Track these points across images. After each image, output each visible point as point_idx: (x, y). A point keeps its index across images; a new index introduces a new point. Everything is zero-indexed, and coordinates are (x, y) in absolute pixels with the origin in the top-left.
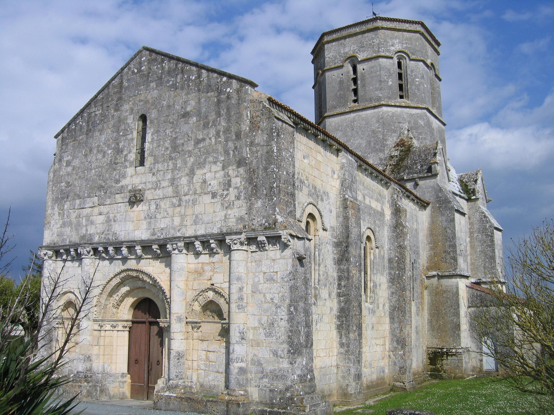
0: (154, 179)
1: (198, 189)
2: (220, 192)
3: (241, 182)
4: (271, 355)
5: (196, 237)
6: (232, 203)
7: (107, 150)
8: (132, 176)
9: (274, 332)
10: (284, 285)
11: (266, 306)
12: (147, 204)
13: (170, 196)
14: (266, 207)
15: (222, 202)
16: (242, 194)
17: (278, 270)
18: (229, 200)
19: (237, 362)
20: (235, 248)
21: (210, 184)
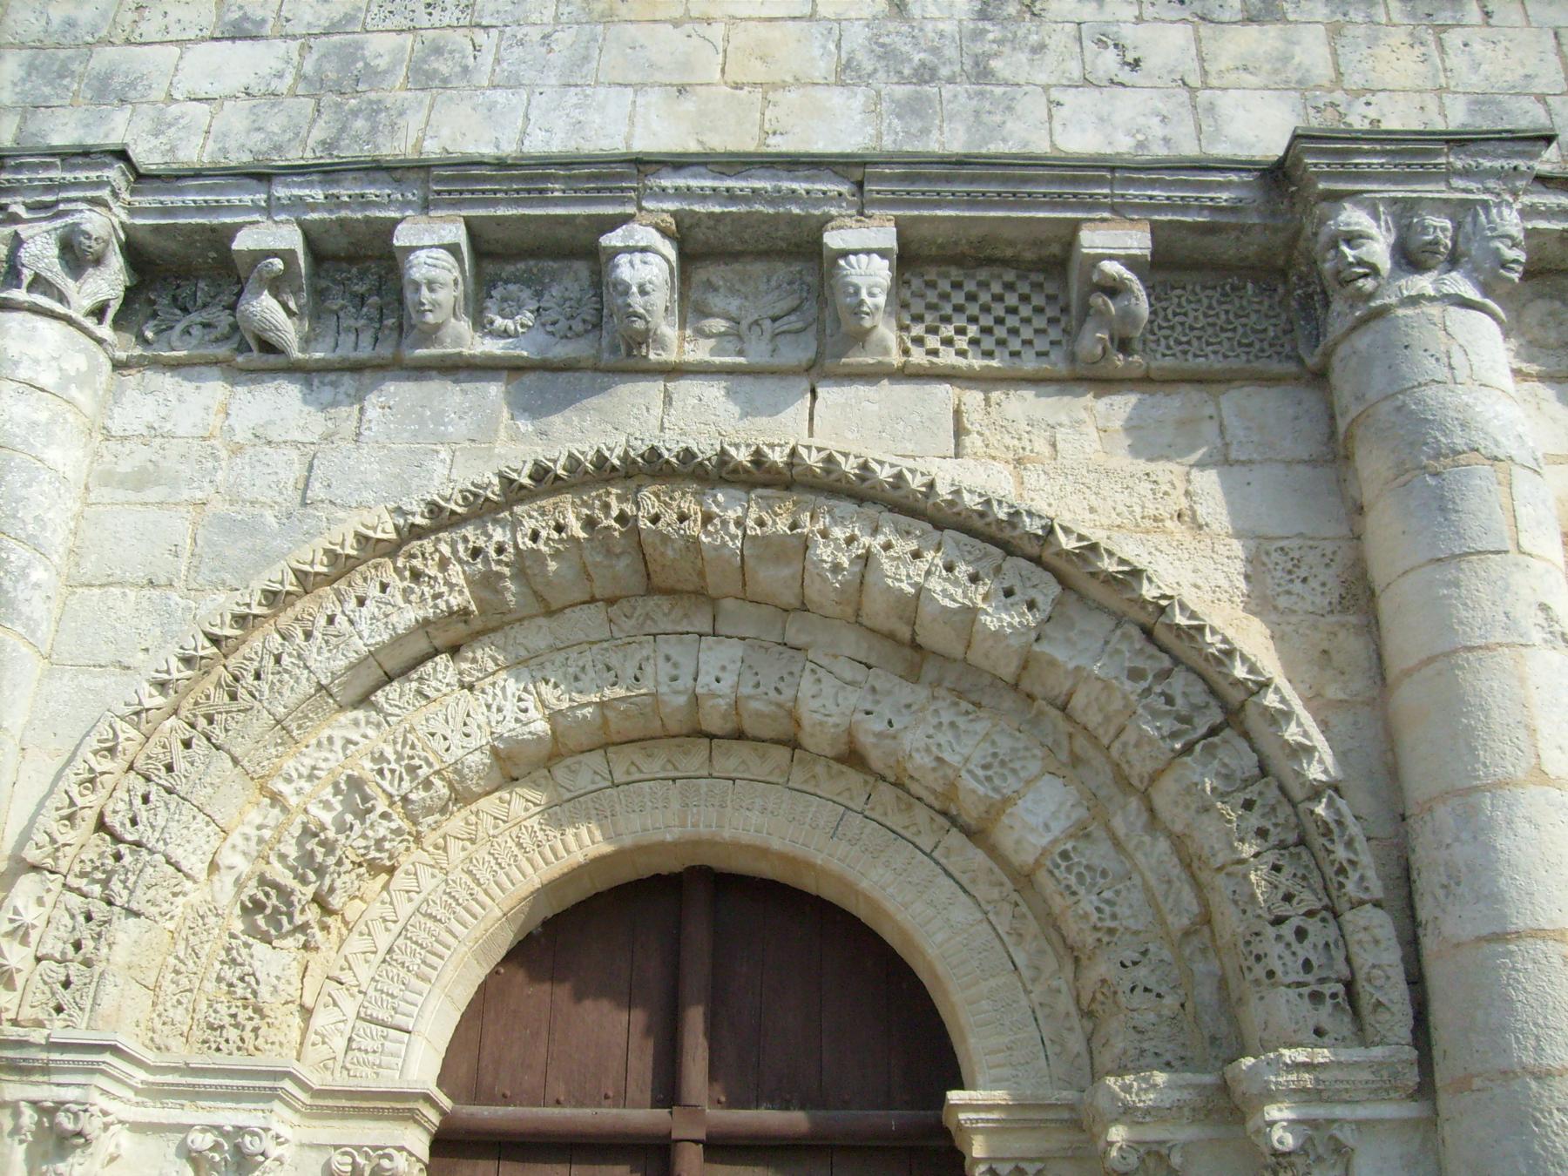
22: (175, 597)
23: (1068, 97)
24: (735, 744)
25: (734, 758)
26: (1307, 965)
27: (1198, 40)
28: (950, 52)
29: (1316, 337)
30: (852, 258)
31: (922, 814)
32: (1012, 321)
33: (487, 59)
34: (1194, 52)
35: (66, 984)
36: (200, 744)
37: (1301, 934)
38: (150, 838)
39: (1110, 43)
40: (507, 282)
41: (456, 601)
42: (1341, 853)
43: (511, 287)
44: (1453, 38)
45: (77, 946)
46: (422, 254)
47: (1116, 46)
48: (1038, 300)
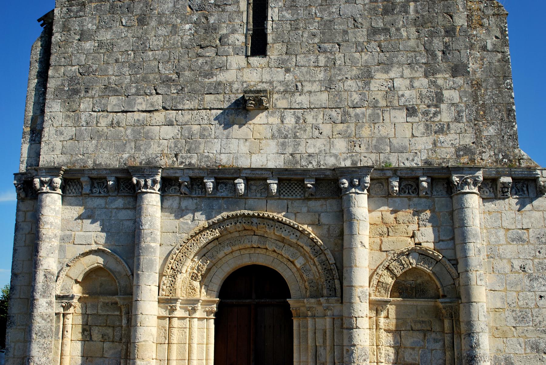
0: (289, 77)
1: (380, 100)
2: (423, 107)
3: (460, 98)
4: (528, 351)
5: (395, 171)
6: (446, 126)
9: (530, 315)
10: (542, 248)
11: (512, 277)
12: (278, 114)
13: (324, 106)
14: (503, 137)
15: (428, 123)
16: (464, 114)
17: (530, 226)
18: (440, 120)
19: (485, 361)
20: (468, 190)
21: (403, 95)
22: (177, 234)
23: (309, 141)
24: (258, 249)
25: (259, 251)
26: (330, 286)
27: (332, 127)
28: (290, 132)
29: (341, 193)
31: (285, 259)
32: (296, 190)
33: (213, 132)
35: (171, 290)
36: (184, 257)
37: (329, 282)
38: (179, 270)
41: (218, 235)
42: (334, 273)
44: (377, 126)
45: (172, 285)
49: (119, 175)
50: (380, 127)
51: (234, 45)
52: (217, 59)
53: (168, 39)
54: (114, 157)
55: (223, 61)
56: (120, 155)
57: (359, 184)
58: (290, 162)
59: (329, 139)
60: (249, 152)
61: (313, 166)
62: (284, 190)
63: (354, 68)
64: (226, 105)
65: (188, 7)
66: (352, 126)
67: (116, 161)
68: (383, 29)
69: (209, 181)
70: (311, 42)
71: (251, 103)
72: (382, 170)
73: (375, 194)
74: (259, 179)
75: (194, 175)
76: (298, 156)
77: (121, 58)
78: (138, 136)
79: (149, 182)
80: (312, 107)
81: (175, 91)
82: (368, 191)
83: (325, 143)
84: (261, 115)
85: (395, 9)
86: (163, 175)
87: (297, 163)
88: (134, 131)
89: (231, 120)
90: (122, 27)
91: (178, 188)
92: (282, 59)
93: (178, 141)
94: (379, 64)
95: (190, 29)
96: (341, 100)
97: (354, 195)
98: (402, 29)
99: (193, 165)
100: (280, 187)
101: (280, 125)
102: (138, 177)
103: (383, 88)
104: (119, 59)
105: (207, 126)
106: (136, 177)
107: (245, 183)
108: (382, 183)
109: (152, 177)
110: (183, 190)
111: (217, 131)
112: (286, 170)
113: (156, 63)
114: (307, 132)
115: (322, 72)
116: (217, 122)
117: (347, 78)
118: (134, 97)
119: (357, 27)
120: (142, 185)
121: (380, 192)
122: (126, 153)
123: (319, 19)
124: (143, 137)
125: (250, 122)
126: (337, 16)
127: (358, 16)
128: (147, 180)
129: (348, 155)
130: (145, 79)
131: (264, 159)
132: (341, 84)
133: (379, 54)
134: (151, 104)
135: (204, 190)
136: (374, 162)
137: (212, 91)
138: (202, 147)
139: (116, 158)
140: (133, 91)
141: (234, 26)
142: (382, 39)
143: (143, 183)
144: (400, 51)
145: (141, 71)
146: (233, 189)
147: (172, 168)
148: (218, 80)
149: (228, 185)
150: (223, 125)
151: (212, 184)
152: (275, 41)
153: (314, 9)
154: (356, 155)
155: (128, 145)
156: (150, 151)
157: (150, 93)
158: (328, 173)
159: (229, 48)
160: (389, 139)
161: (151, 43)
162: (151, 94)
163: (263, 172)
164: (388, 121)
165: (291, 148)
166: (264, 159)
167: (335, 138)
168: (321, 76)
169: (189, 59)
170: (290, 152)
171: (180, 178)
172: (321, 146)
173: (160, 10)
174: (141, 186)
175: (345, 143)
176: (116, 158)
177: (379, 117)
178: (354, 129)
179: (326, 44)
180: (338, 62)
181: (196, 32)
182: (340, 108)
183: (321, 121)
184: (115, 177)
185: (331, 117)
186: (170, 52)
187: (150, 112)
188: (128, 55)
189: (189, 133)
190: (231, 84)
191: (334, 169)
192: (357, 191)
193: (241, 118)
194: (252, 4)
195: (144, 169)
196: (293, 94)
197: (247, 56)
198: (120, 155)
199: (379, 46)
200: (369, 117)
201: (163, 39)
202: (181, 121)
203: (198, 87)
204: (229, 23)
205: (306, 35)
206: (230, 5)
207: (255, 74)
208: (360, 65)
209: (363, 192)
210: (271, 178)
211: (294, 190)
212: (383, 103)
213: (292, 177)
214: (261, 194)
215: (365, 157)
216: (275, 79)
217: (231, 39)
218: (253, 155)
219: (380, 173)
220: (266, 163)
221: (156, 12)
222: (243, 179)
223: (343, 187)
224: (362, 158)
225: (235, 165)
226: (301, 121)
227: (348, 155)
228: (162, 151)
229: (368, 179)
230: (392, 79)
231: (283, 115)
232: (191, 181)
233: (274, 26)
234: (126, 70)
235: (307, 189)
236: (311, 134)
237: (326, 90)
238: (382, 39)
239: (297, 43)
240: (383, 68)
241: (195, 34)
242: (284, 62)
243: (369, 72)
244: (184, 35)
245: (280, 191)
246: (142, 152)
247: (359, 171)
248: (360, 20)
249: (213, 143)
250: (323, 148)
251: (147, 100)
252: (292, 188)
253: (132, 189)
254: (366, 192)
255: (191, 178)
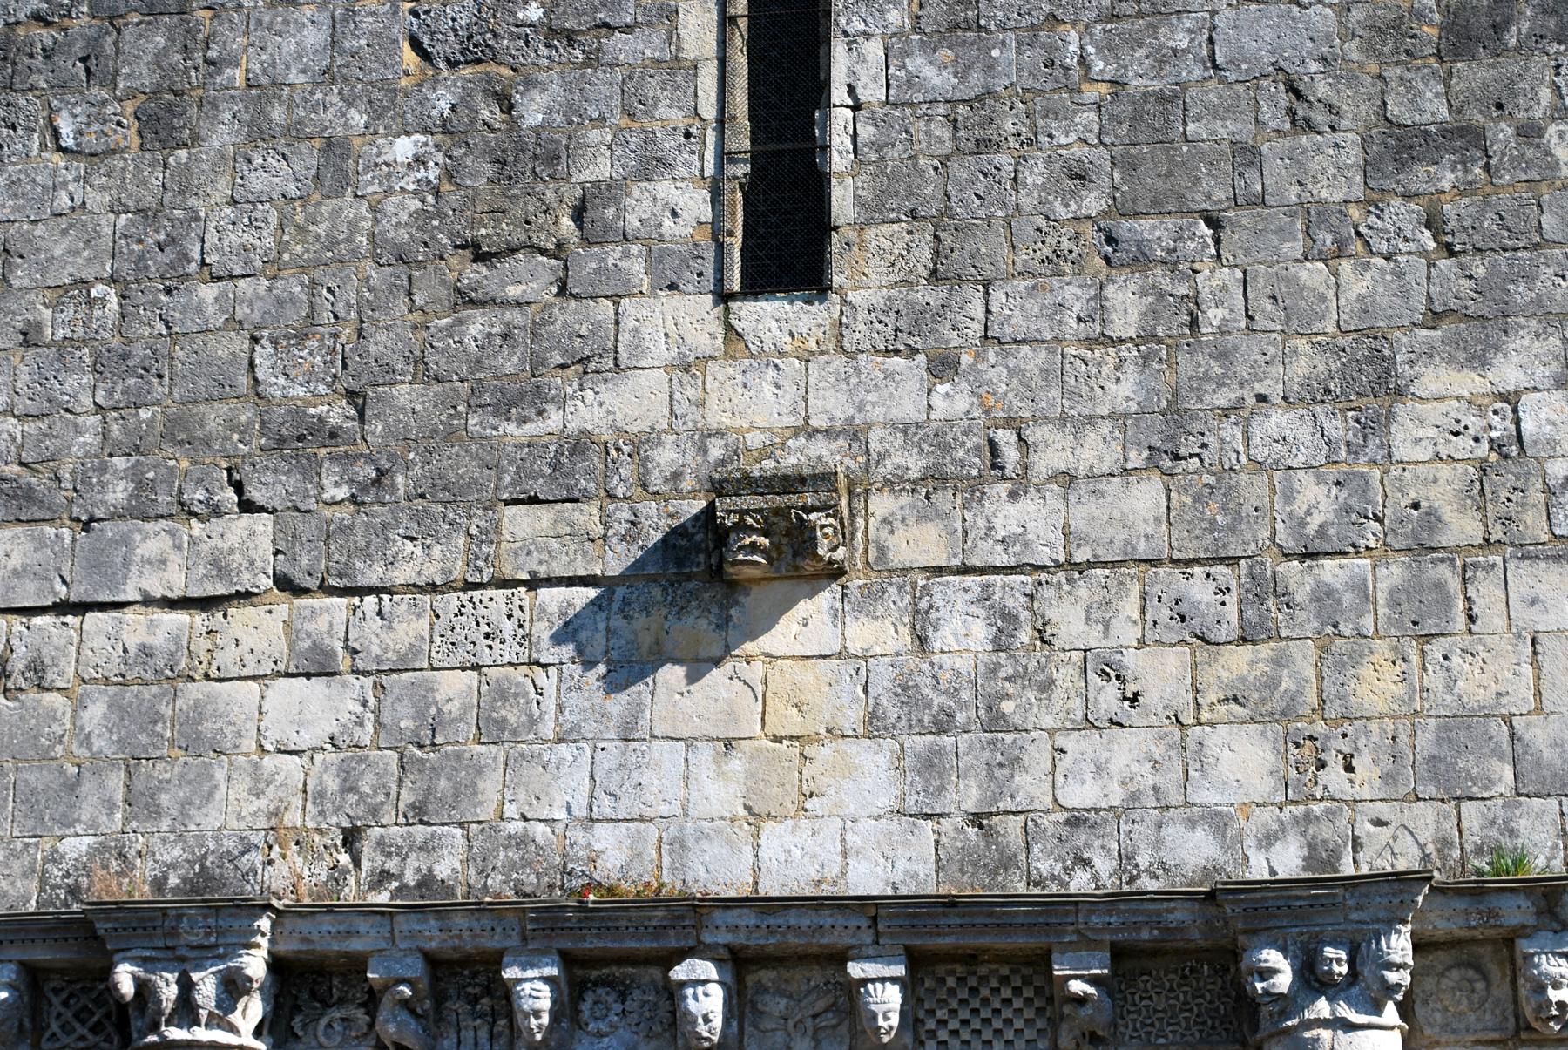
0: (952, 401)
1: (1447, 513)
7: (370, 131)
8: (686, 366)
12: (896, 600)
13: (1142, 550)
23: (1068, 742)
27: (1194, 666)
28: (966, 695)
29: (1255, 1028)
30: (870, 986)
32: (1007, 1013)
33: (550, 705)
34: (1189, 681)
39: (1112, 674)
40: (596, 984)
43: (601, 991)
44: (1435, 650)
46: (527, 986)
47: (1118, 677)
48: (1028, 992)
49: (40, 954)
50: (1456, 660)
51: (652, 241)
52: (567, 315)
53: (300, 218)
54: (14, 854)
55: (597, 326)
56: (47, 844)
57: (1354, 974)
58: (967, 859)
59: (1176, 730)
60: (748, 808)
61: (1095, 877)
62: (941, 1014)
63: (1301, 343)
64: (616, 561)
65: (406, 47)
66: (1304, 659)
67: (25, 875)
68: (1448, 133)
69: (530, 973)
70: (1061, 212)
71: (753, 548)
72: (1475, 891)
73: (1445, 1027)
74: (803, 959)
75: (450, 943)
76: (1012, 828)
77: (54, 324)
78: (143, 738)
79: (207, 987)
80: (1080, 556)
81: (342, 493)
82: (1405, 1010)
83: (1158, 751)
84: (804, 607)
85: (1507, 22)
86: (283, 948)
87: (1007, 862)
88: (121, 708)
89: (646, 640)
90: (58, 159)
91: (361, 1016)
92: (911, 306)
93: (361, 760)
94: (1435, 318)
95: (419, 161)
96: (1237, 518)
97: (1325, 1034)
98: (1552, 129)
99: (446, 888)
100: (920, 1001)
101: (912, 661)
102: (143, 962)
103: (1465, 442)
104: (39, 326)
105: (518, 675)
106: (132, 960)
107: (729, 979)
108: (1478, 968)
109: (222, 958)
110: (391, 1028)
111: (573, 699)
112: (950, 903)
113: (241, 343)
114: (1058, 695)
115: (1130, 368)
116: (568, 650)
117: (1262, 398)
118: (124, 526)
119: (1310, 127)
120: (168, 1006)
121: (1472, 1017)
122: (79, 828)
123: (1104, 88)
124: (172, 741)
125: (749, 647)
126: (1197, 73)
127: (1313, 67)
128: (195, 977)
129: (1286, 815)
130: (178, 431)
131: (829, 845)
132: (1232, 432)
133: (1431, 265)
134: (215, 563)
135: (502, 1022)
136: (1430, 849)
137: (539, 487)
138: (489, 787)
139: (26, 859)
140: (118, 493)
141: (649, 138)
142: (1446, 185)
143: (169, 992)
144: (1546, 243)
145: (159, 390)
146: (663, 1013)
147: (330, 909)
148: (573, 426)
149: (637, 994)
150: (601, 669)
151: (545, 990)
152: (872, 213)
153: (1073, 36)
154: (1327, 811)
155: (86, 787)
156: (210, 819)
157: (207, 502)
158: (1180, 914)
159: (626, 255)
160: (1508, 719)
161: (211, 238)
162: (216, 511)
163: (826, 918)
164: (1499, 622)
165: (972, 782)
166: (829, 845)
167: (1212, 725)
168: (1124, 390)
169: (417, 317)
170: (970, 805)
171: (372, 962)
172: (1135, 767)
173: (256, 67)
174: (160, 1012)
175: (1268, 747)
176: (26, 859)
177: (1446, 603)
178: (1311, 672)
179: (1145, 224)
180: (1214, 316)
181: (449, 174)
182: (1232, 561)
183: (1131, 635)
184: (22, 964)
185: (1184, 607)
186: (314, 283)
187: (206, 604)
188: (91, 302)
189: (420, 714)
190: (641, 446)
191: (1211, 896)
192: (1345, 1011)
193: (698, 625)
194: (743, 24)
195: (179, 917)
196: (974, 489)
197: (723, 297)
198: (47, 844)
199: (1433, 222)
200: (1394, 603)
201: (274, 219)
202: (376, 649)
203: (467, 468)
204: (624, 122)
205: (1034, 176)
206: (628, 29)
207: (768, 390)
208: (1331, 328)
209: (1374, 1019)
210: (871, 951)
211: (997, 1012)
212: (1462, 527)
213: (985, 941)
214: (815, 1037)
215: (1379, 823)
216: (877, 414)
217: (639, 206)
218: (768, 827)
219: (1467, 913)
220: (835, 870)
221: (239, 75)
222: (718, 962)
223: (1266, 992)
224: (1365, 828)
225: (672, 883)
226: (1025, 635)
227: (1286, 815)
228: (276, 813)
229: (1400, 946)
230: (1511, 399)
231: (923, 604)
232: (435, 979)
233: (866, 132)
234: (78, 385)
235: (1067, 1009)
236: (1077, 703)
237: (1152, 464)
238: (1446, 185)
239: (989, 219)
240: (1457, 341)
241: (446, 187)
242: (921, 320)
243: (1383, 363)
244: (389, 192)
245: (918, 1022)
246: (165, 825)
247: (1351, 902)
248: (1322, 89)
249: (551, 767)
250: (1150, 781)
251: (193, 542)
252: (985, 1001)
253: (110, 1029)
254: (1390, 1014)
255: (433, 961)
